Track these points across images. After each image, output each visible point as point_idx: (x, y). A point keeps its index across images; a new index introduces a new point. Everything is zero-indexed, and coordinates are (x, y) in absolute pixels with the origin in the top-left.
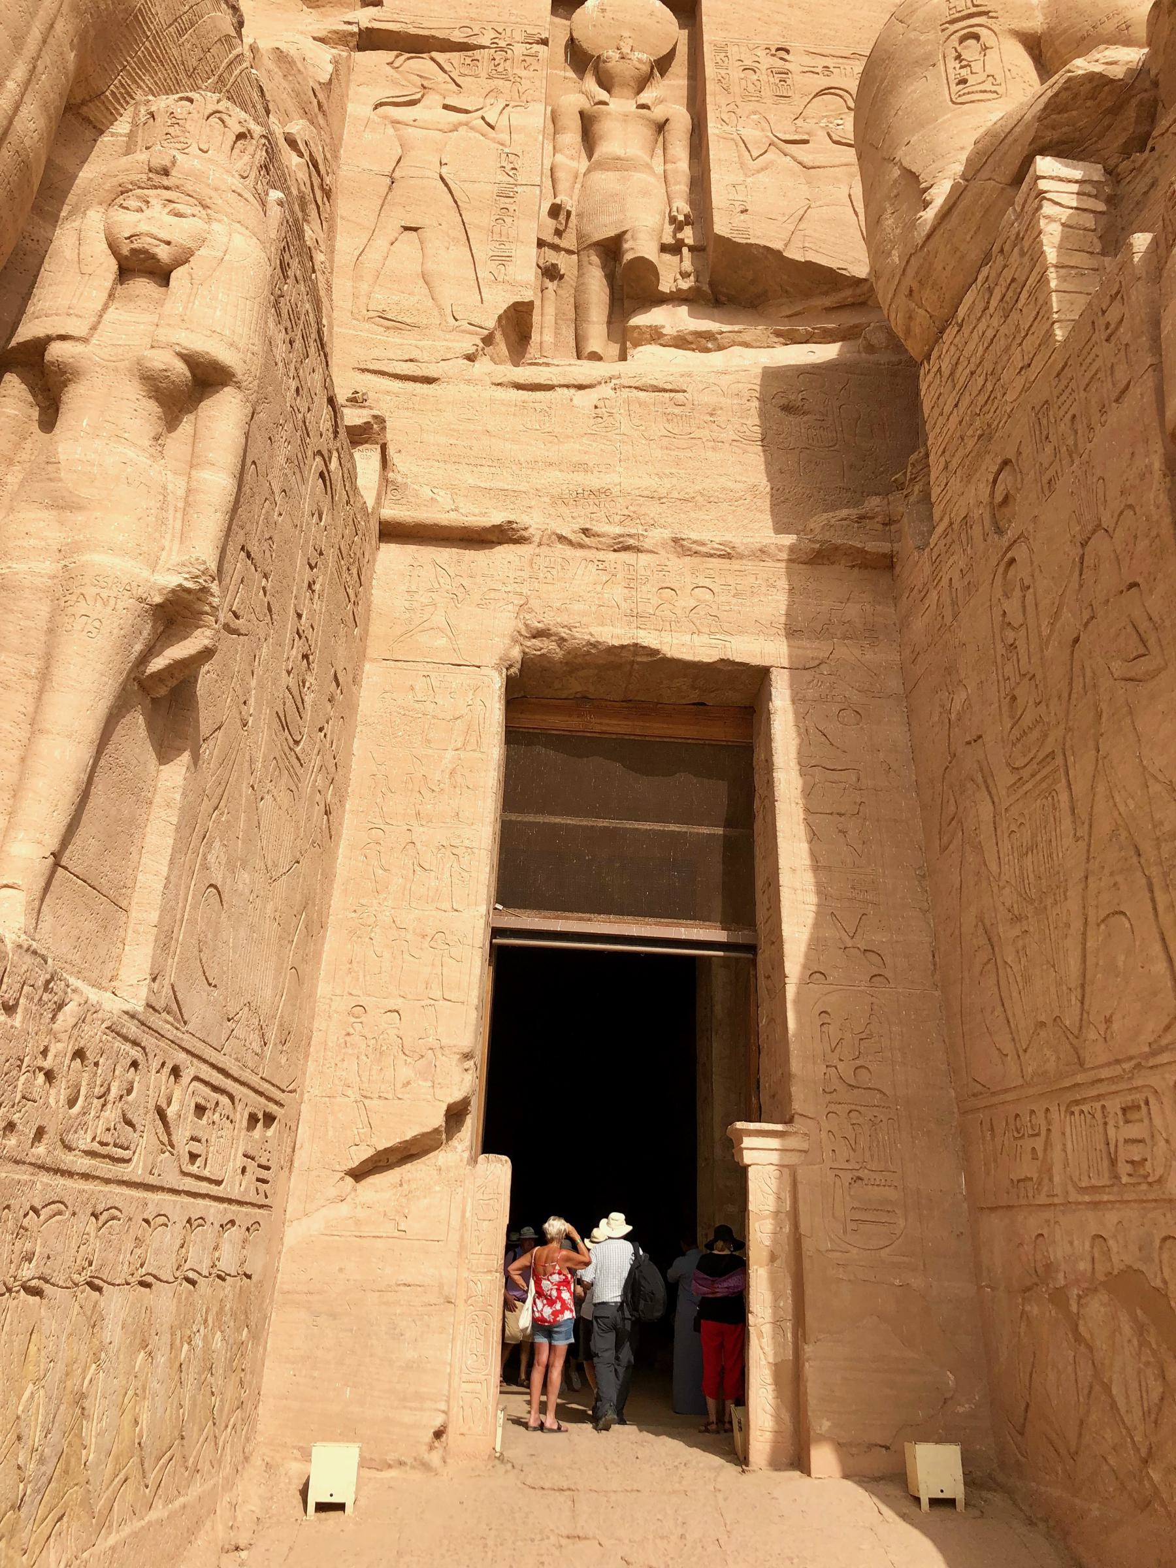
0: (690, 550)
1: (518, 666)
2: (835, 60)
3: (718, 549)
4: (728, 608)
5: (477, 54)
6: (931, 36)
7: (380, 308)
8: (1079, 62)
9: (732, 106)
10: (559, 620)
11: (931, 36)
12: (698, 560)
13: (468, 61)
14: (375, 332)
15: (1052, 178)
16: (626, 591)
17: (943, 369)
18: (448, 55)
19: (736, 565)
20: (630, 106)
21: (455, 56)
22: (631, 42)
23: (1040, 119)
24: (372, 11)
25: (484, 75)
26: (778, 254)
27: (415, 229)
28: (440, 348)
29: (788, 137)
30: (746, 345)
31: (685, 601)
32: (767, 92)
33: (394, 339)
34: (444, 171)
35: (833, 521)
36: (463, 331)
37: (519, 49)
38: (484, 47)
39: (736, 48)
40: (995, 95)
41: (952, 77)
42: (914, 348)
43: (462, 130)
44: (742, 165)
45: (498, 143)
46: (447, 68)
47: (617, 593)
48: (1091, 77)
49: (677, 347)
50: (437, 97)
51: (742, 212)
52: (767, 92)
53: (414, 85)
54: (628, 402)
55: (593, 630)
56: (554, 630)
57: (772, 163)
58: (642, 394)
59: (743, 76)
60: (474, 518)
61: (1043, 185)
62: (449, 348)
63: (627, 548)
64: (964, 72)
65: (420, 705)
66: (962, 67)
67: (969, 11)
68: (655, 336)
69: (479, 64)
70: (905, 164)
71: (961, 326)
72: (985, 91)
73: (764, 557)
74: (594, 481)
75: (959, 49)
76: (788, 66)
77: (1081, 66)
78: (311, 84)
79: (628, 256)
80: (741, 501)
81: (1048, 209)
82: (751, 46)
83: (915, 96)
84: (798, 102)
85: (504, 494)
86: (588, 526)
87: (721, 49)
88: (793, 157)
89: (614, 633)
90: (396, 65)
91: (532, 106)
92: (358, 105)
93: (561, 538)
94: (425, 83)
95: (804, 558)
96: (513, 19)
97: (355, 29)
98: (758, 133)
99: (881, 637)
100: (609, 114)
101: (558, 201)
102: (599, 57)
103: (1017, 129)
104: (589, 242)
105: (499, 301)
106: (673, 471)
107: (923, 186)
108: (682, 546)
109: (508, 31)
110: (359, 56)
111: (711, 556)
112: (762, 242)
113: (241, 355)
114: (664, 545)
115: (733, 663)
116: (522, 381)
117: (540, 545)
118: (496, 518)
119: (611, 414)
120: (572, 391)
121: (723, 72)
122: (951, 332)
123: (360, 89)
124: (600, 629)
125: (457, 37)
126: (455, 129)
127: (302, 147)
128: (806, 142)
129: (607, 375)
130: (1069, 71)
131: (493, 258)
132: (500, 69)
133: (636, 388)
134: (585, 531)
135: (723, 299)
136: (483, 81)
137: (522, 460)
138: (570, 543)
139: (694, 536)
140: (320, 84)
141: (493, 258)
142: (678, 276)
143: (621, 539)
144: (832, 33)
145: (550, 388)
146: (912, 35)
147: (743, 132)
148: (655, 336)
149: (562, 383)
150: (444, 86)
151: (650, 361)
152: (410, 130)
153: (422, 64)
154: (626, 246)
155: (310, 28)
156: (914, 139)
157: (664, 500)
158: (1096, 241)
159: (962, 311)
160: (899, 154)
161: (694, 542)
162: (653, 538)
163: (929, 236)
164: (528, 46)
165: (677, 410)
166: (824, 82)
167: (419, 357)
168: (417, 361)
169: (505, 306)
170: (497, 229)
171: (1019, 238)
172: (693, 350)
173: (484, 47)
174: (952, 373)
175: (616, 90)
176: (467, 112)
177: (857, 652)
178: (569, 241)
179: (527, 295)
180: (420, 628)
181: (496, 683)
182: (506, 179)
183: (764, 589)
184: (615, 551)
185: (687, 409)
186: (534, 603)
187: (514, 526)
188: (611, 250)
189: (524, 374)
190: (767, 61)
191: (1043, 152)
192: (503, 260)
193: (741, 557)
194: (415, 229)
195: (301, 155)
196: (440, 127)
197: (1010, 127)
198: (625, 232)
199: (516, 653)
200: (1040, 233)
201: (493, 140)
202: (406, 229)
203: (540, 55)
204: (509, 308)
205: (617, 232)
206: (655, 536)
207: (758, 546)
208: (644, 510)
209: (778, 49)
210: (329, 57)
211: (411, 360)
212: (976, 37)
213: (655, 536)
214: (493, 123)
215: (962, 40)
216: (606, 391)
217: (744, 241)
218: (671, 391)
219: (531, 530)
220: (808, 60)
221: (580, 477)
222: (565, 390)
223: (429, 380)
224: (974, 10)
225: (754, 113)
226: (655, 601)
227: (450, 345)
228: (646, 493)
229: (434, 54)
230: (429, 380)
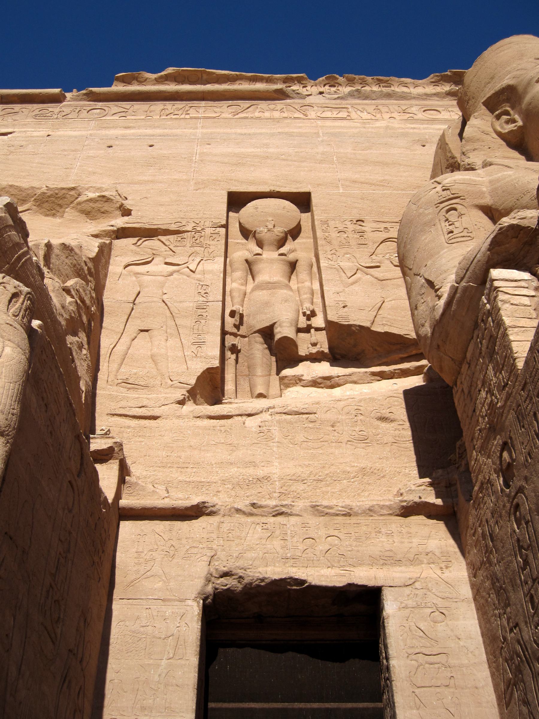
0: (323, 512)
1: (211, 597)
2: (391, 224)
3: (341, 511)
4: (350, 549)
5: (185, 235)
6: (430, 210)
7: (124, 378)
8: (504, 219)
9: (332, 252)
10: (237, 565)
11: (430, 210)
12: (327, 518)
13: (179, 239)
14: (122, 391)
15: (502, 280)
16: (282, 542)
17: (464, 390)
18: (168, 237)
19: (353, 520)
20: (274, 255)
21: (172, 237)
22: (273, 223)
23: (489, 250)
24: (126, 218)
25: (189, 245)
26: (368, 329)
27: (147, 331)
28: (162, 397)
29: (368, 265)
30: (355, 382)
31: (322, 547)
32: (353, 243)
33: (132, 394)
34: (165, 297)
35: (413, 488)
37: (208, 231)
38: (188, 231)
39: (333, 222)
40: (469, 238)
41: (445, 230)
42: (448, 379)
43: (175, 275)
44: (342, 281)
45: (197, 280)
46: (167, 243)
47: (277, 544)
48: (512, 227)
49: (312, 386)
50: (161, 259)
51: (344, 307)
52: (353, 243)
53: (148, 254)
54: (279, 422)
55: (260, 569)
56: (234, 572)
57: (360, 279)
58: (290, 417)
59: (338, 235)
60: (180, 502)
61: (496, 284)
62: (166, 398)
63: (281, 514)
64: (451, 228)
65: (144, 629)
66: (450, 225)
67: (449, 197)
68: (298, 380)
69: (185, 240)
70: (426, 277)
71: (469, 364)
72: (464, 237)
73: (371, 514)
74: (261, 472)
75: (447, 216)
76: (363, 228)
77: (506, 221)
78: (84, 259)
79: (277, 337)
80: (355, 479)
81: (501, 296)
82: (342, 220)
83: (427, 241)
84: (371, 247)
85: (199, 485)
86: (255, 502)
87: (326, 222)
88: (371, 275)
89: (274, 571)
91: (217, 259)
92: (115, 266)
93: (238, 511)
94: (154, 252)
95: (398, 512)
96: (205, 216)
97: (115, 229)
98: (351, 264)
99: (453, 561)
100: (263, 260)
101: (234, 309)
102: (255, 231)
103: (478, 256)
104: (254, 330)
105: (198, 367)
106: (311, 463)
107: (437, 287)
108: (317, 510)
109: (202, 222)
110: (116, 242)
111: (337, 515)
112: (357, 323)
113: (4, 416)
114: (305, 510)
115: (357, 586)
116: (213, 414)
117: (224, 515)
118: (195, 500)
119: (269, 431)
120: (244, 418)
121: (327, 234)
122: (465, 367)
123: (117, 258)
124: (265, 569)
125: (173, 227)
126: (171, 274)
127: (73, 293)
128: (378, 267)
129: (266, 407)
130: (500, 224)
131: (193, 344)
132: (198, 242)
133: (285, 413)
134: (253, 505)
135: (338, 357)
136: (187, 248)
137: (213, 462)
138: (244, 513)
139: (325, 503)
140: (90, 258)
141: (193, 344)
142: (310, 346)
143: (277, 508)
144: (387, 211)
146: (421, 211)
147: (341, 264)
148: (298, 380)
149: (237, 413)
150: (165, 253)
151: (297, 397)
152: (146, 278)
153: (154, 243)
154: (276, 331)
155: (90, 230)
156: (429, 263)
157: (305, 481)
158: (532, 311)
159: (469, 355)
160: (422, 272)
161: (325, 507)
162: (298, 506)
163: (443, 314)
164: (214, 229)
165: (311, 425)
166: (385, 235)
167: (148, 405)
168: (147, 407)
169: (201, 371)
171: (489, 313)
172: (322, 388)
173: (188, 231)
174: (469, 392)
175: (265, 247)
176: (178, 265)
177: (439, 572)
178: (243, 330)
179: (216, 363)
180: (145, 576)
181: (194, 610)
182: (202, 299)
183: (373, 535)
184: (274, 516)
185: (317, 424)
186: (221, 555)
187: (206, 505)
188: (267, 333)
189: (217, 409)
190: (351, 227)
191: (495, 267)
192: (199, 344)
193: (356, 514)
194: (147, 331)
195: (72, 297)
196: (162, 274)
197: (475, 255)
198: (275, 323)
199: (210, 589)
200: (499, 309)
201: (194, 278)
202: (142, 331)
203: (220, 233)
204: (204, 372)
205: (271, 323)
206: (300, 505)
207: (368, 507)
208: (293, 488)
209: (357, 221)
210: (97, 244)
211: (143, 407)
212: (455, 209)
213: (300, 505)
214: (194, 270)
215: (448, 211)
216: (266, 416)
217: (347, 323)
218: (307, 413)
219: (217, 507)
220: (375, 225)
221: (251, 471)
222: (240, 418)
223: (155, 418)
224: (452, 196)
225: (347, 253)
226: (301, 547)
227: (167, 396)
228: (294, 477)
229: (160, 237)
230: (155, 418)
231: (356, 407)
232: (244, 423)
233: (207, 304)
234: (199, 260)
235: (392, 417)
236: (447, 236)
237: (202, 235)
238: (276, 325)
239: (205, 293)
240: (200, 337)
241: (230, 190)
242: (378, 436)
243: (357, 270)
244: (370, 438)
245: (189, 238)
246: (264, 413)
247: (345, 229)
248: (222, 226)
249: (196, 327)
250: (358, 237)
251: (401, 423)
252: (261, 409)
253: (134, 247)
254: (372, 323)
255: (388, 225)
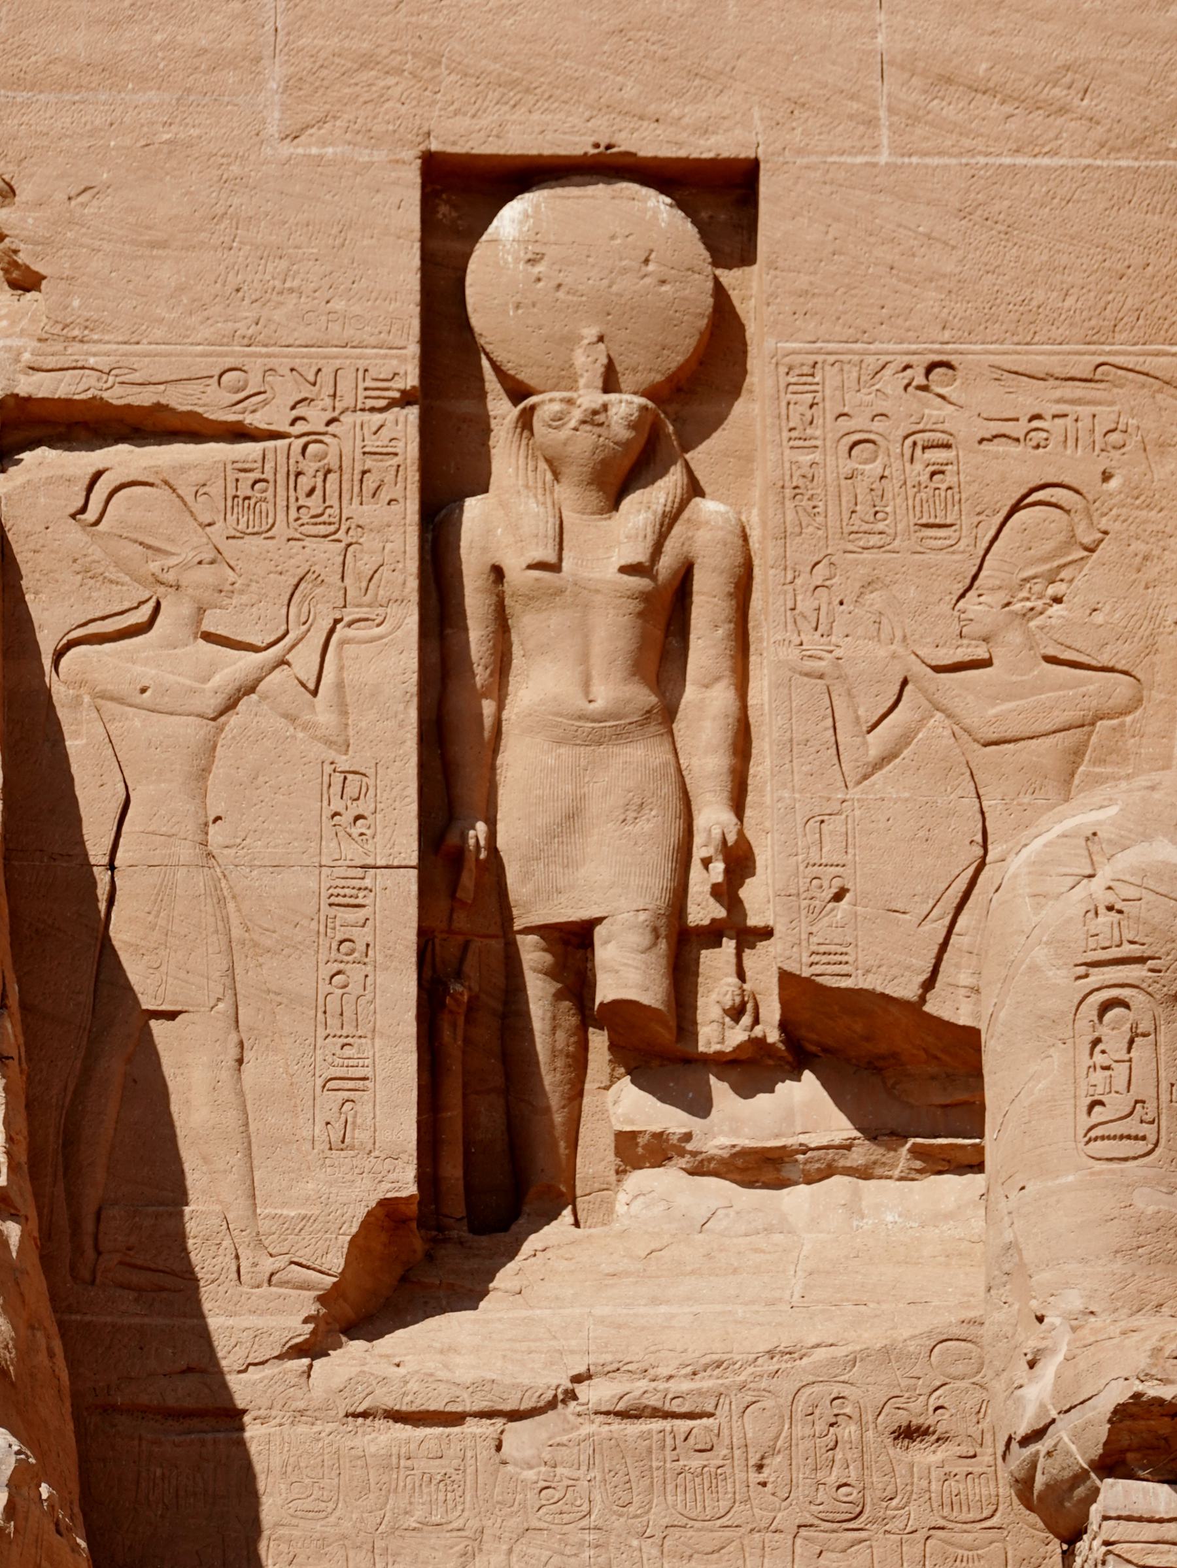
13: (244, 490)
32: (899, 513)
36: (282, 1284)
40: (1141, 1147)
82: (872, 362)
90: (91, 515)
120: (499, 1422)
121: (806, 458)
125: (215, 405)
135: (814, 1049)
145: (454, 1419)
149: (475, 1408)
164: (377, 418)
165: (696, 1462)
169: (361, 1212)
170: (333, 1005)
198: (599, 920)
231: (836, 1390)
232: (499, 1448)
233: (367, 882)
234: (327, 624)
235: (941, 1429)
236: (1085, 1122)
237: (332, 461)
238: (599, 932)
239: (358, 818)
240: (348, 1051)
241: (435, 146)
242: (894, 1503)
243: (905, 682)
244: (868, 1508)
245: (281, 478)
246: (560, 1406)
247: (877, 425)
248: (406, 399)
249: (333, 1005)
250: (924, 478)
251: (965, 1450)
252: (549, 1395)
253: (74, 535)
254: (929, 984)
255: (1045, 399)
